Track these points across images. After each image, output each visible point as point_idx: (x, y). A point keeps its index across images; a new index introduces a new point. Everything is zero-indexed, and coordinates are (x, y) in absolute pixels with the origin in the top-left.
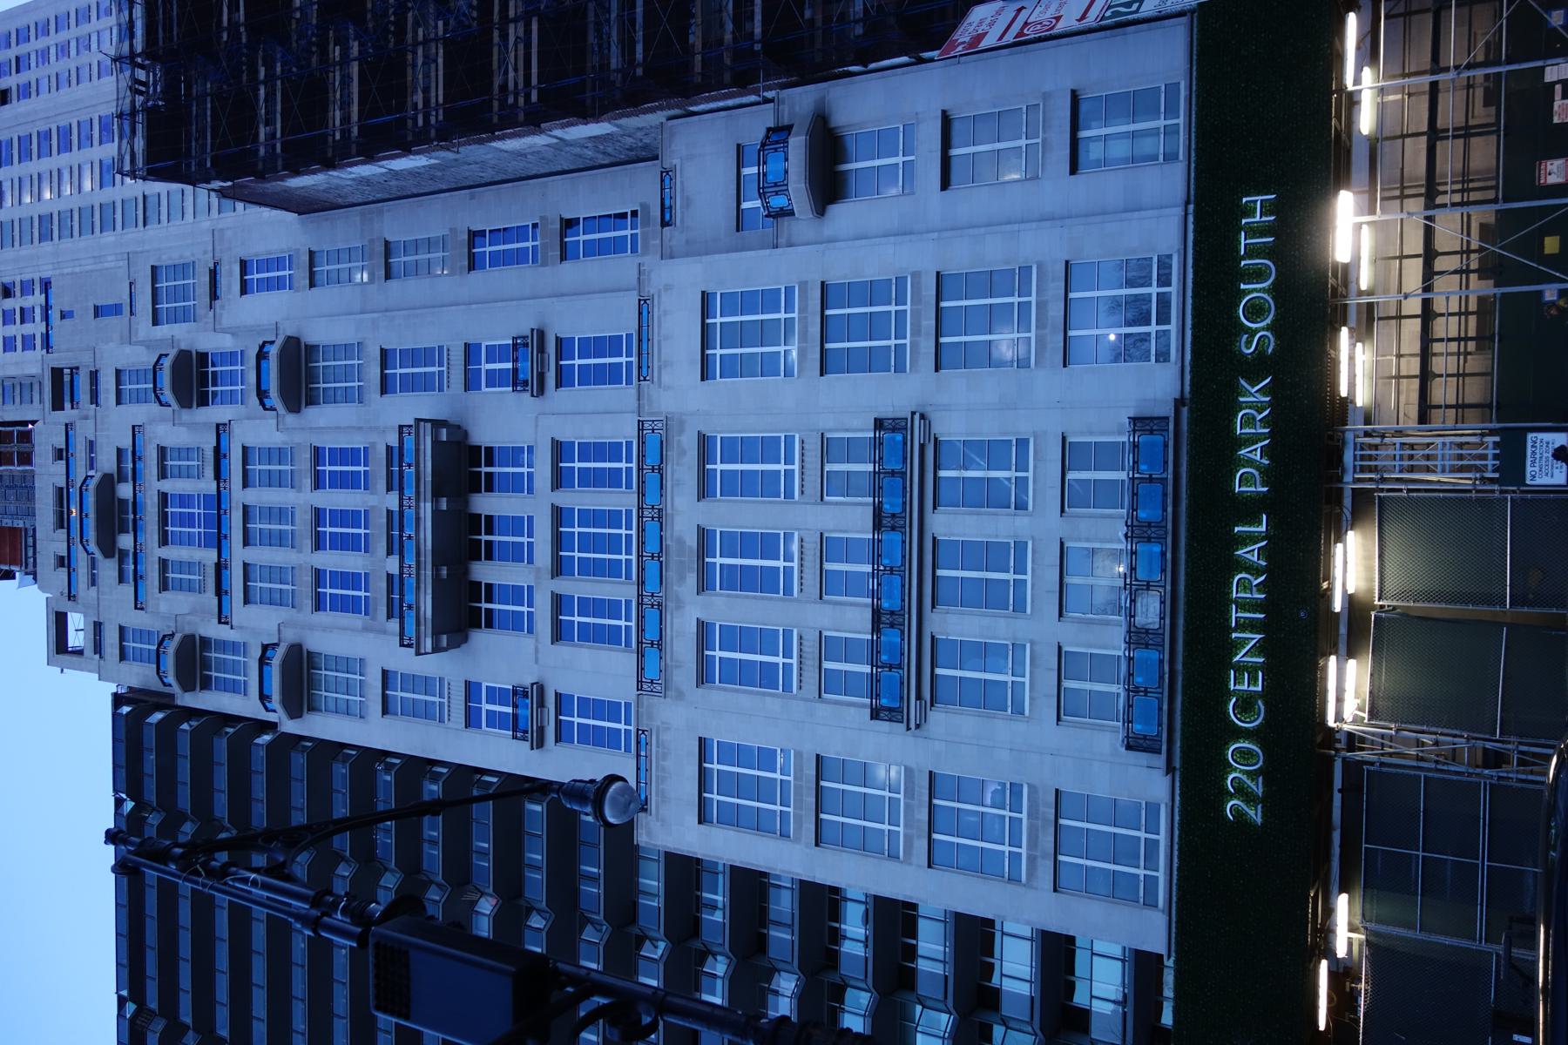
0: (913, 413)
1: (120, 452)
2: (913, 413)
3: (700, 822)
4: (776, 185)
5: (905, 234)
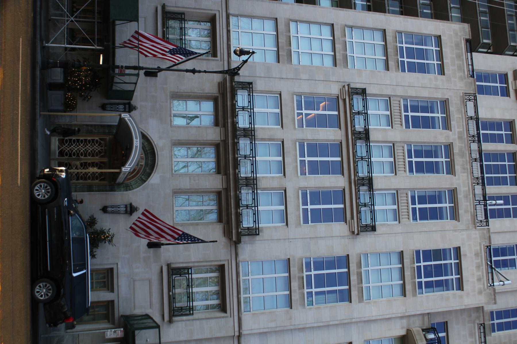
0: (358, 234)
3: (440, 36)
5: (368, 321)
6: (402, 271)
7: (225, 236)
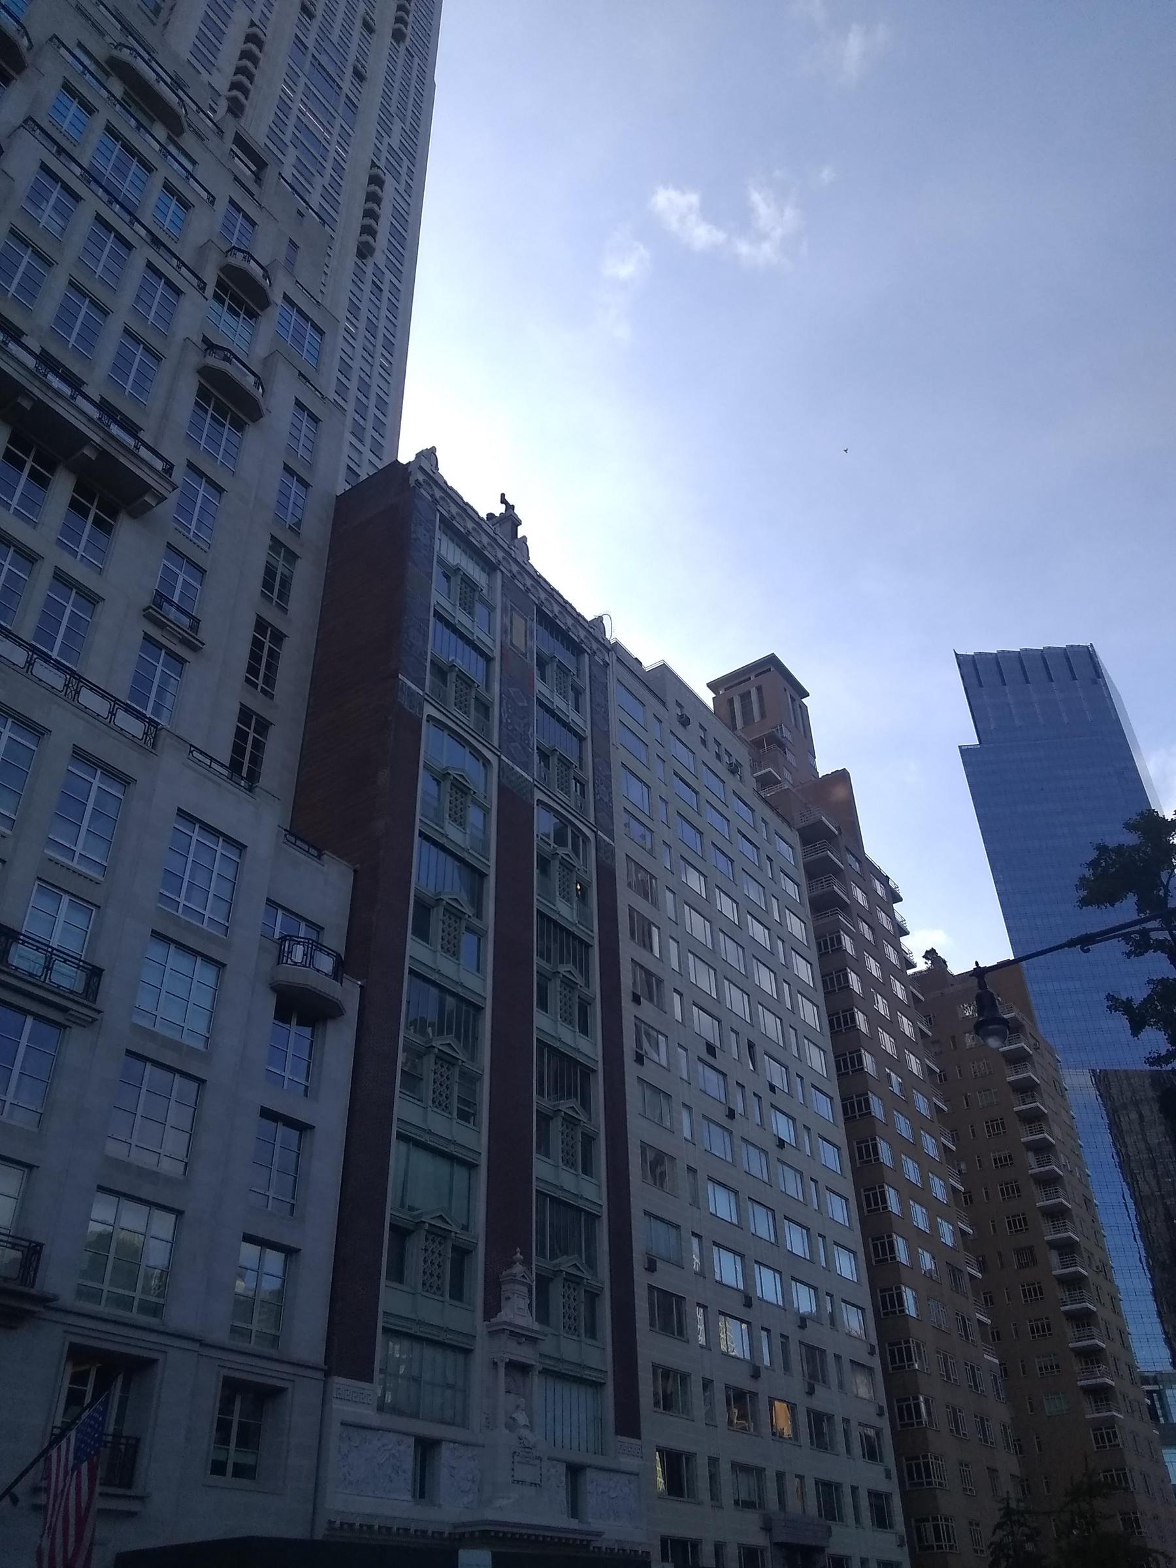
1: (194, 162)
2: (99, 1012)
4: (312, 957)
6: (181, 946)
7: (11, 1328)
